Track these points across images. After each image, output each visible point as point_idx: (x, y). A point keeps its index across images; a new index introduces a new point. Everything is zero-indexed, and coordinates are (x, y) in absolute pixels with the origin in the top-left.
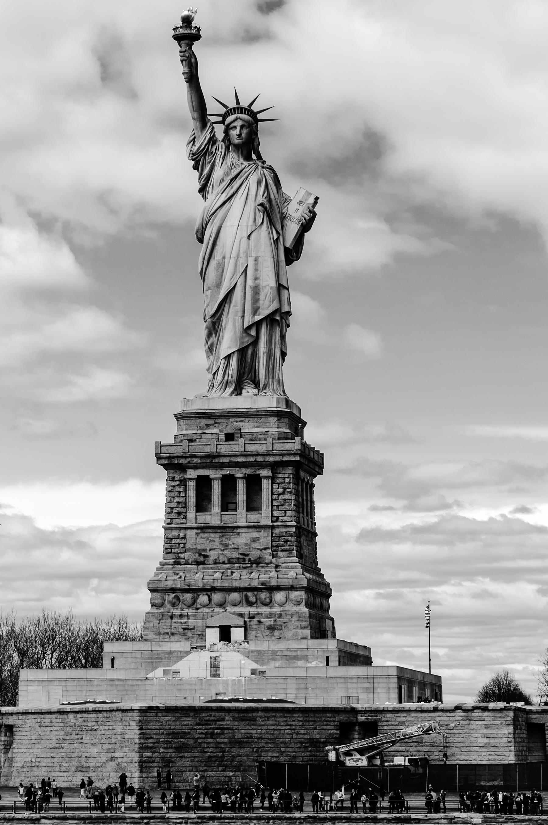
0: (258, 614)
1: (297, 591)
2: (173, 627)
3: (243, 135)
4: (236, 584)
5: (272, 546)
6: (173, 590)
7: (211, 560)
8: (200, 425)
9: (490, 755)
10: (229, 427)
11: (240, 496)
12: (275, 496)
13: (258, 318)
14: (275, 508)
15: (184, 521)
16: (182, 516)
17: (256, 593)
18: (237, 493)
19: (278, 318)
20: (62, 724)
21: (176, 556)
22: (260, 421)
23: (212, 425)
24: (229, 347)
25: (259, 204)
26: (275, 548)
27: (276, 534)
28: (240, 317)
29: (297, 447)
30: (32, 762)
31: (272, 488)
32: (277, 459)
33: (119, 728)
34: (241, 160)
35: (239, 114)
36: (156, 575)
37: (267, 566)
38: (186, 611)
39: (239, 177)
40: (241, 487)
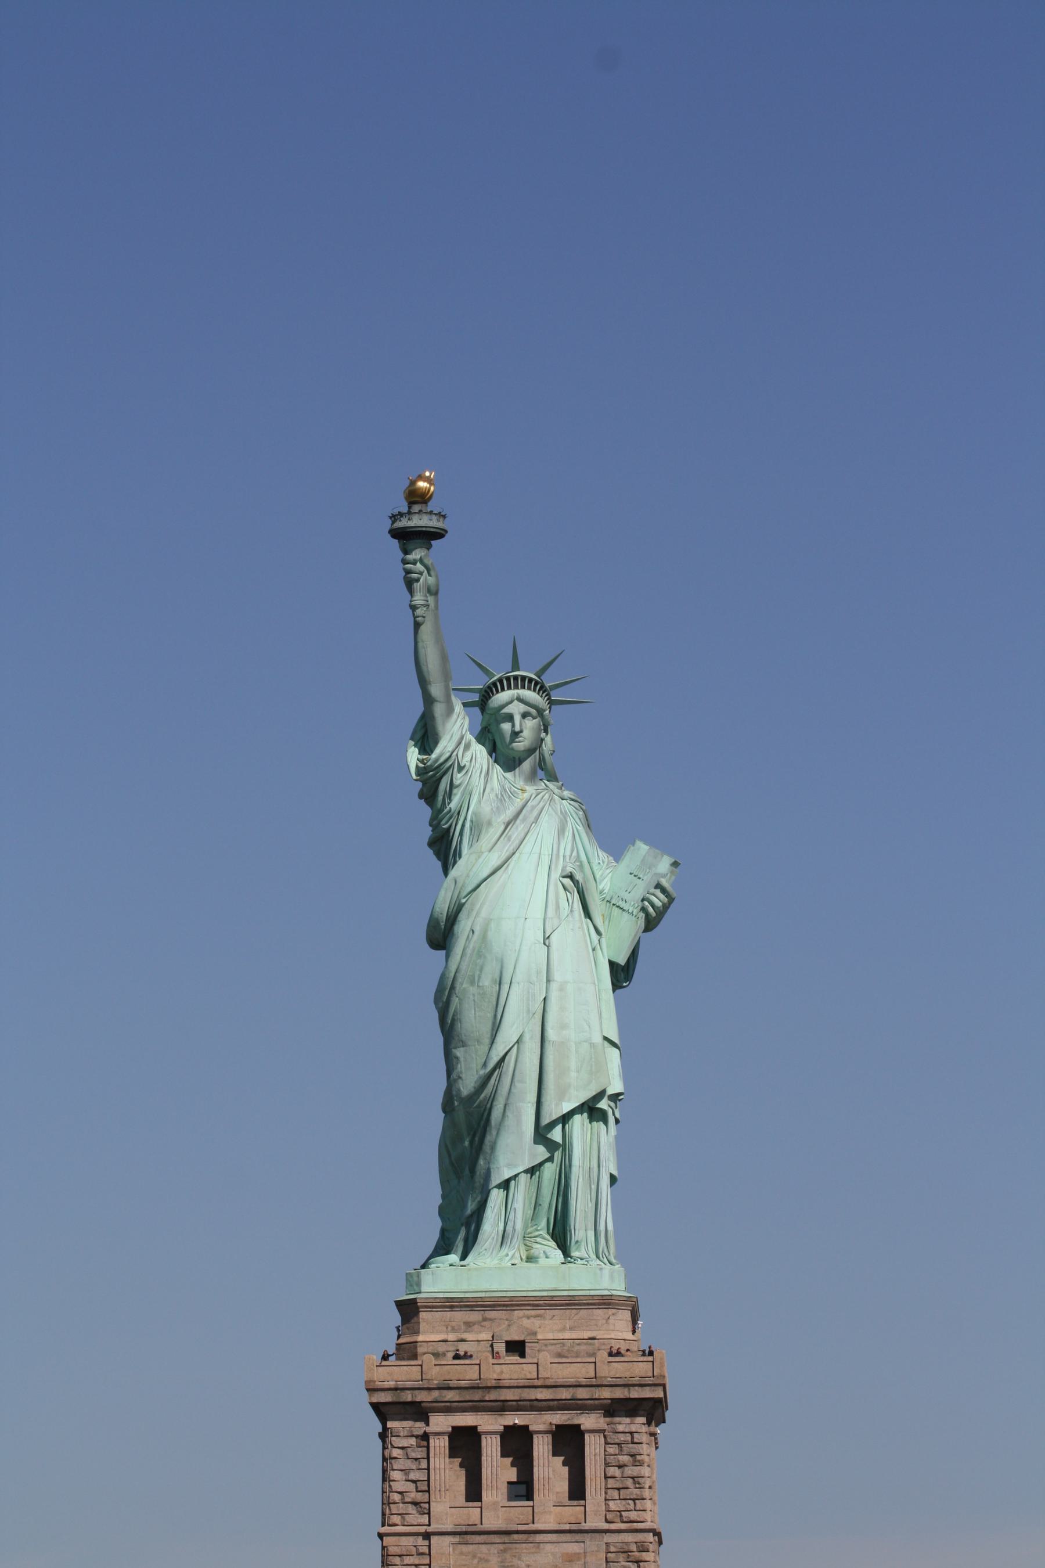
3: (526, 733)
8: (454, 1324)
10: (514, 1328)
11: (541, 1468)
13: (567, 1107)
15: (425, 1519)
18: (535, 1463)
23: (479, 1323)
25: (564, 874)
27: (615, 1546)
28: (530, 1105)
29: (659, 1371)
32: (619, 1393)
34: (520, 783)
35: (518, 689)
39: (521, 817)
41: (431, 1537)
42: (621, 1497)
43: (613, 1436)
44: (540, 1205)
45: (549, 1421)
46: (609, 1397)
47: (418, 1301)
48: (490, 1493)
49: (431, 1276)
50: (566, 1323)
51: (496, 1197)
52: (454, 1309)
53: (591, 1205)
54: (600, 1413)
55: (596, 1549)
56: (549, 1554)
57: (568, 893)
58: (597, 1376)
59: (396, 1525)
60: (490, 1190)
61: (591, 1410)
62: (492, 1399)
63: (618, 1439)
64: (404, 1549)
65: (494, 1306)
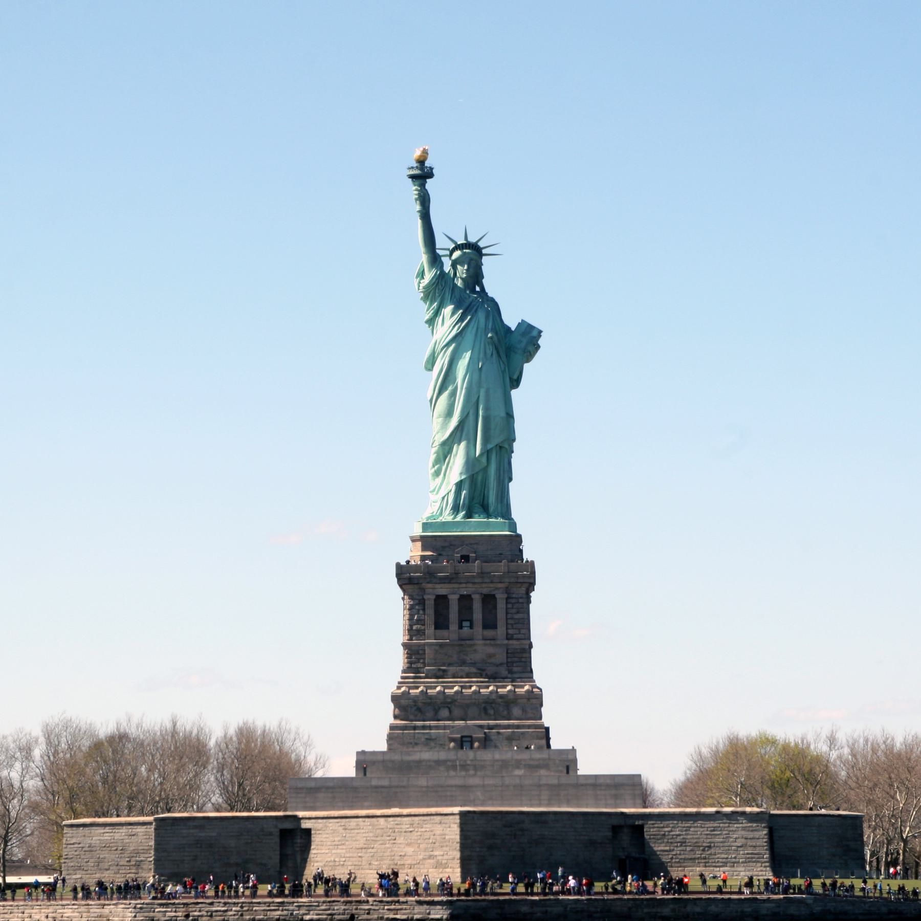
2: (416, 737)
5: (507, 662)
9: (748, 854)
12: (509, 616)
13: (489, 446)
14: (510, 626)
16: (421, 634)
17: (493, 705)
19: (507, 446)
20: (371, 827)
24: (461, 474)
30: (335, 861)
31: (507, 608)
32: (513, 580)
33: (438, 830)
36: (399, 688)
40: (477, 606)
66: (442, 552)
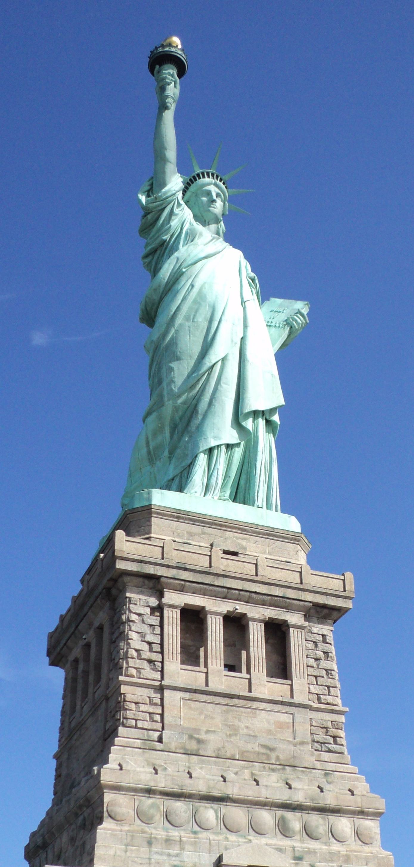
0: (309, 852)
1: (367, 819)
2: (153, 861)
4: (264, 794)
6: (149, 792)
7: (210, 750)
8: (179, 531)
10: (229, 541)
11: (256, 649)
17: (298, 814)
18: (251, 644)
21: (143, 734)
22: (274, 546)
23: (199, 535)
26: (315, 744)
37: (310, 772)
38: (175, 833)
41: (165, 690)
42: (319, 683)
43: (310, 635)
44: (230, 477)
45: (262, 613)
46: (312, 601)
47: (153, 507)
48: (214, 661)
49: (160, 494)
50: (266, 548)
51: (202, 459)
52: (180, 520)
53: (266, 486)
54: (301, 614)
55: (303, 721)
56: (264, 720)
57: (252, 288)
58: (303, 582)
59: (132, 676)
60: (198, 453)
61: (295, 611)
62: (219, 585)
63: (314, 637)
64: (139, 698)
65: (212, 524)
66: (189, 541)
